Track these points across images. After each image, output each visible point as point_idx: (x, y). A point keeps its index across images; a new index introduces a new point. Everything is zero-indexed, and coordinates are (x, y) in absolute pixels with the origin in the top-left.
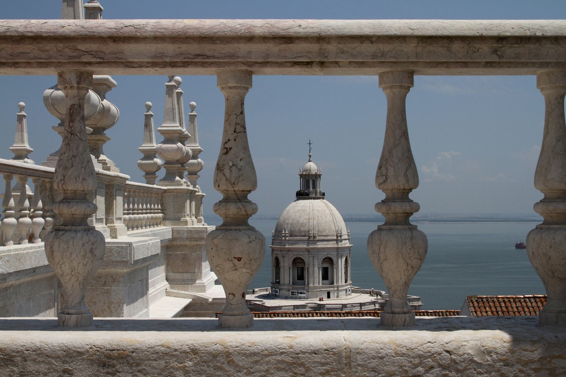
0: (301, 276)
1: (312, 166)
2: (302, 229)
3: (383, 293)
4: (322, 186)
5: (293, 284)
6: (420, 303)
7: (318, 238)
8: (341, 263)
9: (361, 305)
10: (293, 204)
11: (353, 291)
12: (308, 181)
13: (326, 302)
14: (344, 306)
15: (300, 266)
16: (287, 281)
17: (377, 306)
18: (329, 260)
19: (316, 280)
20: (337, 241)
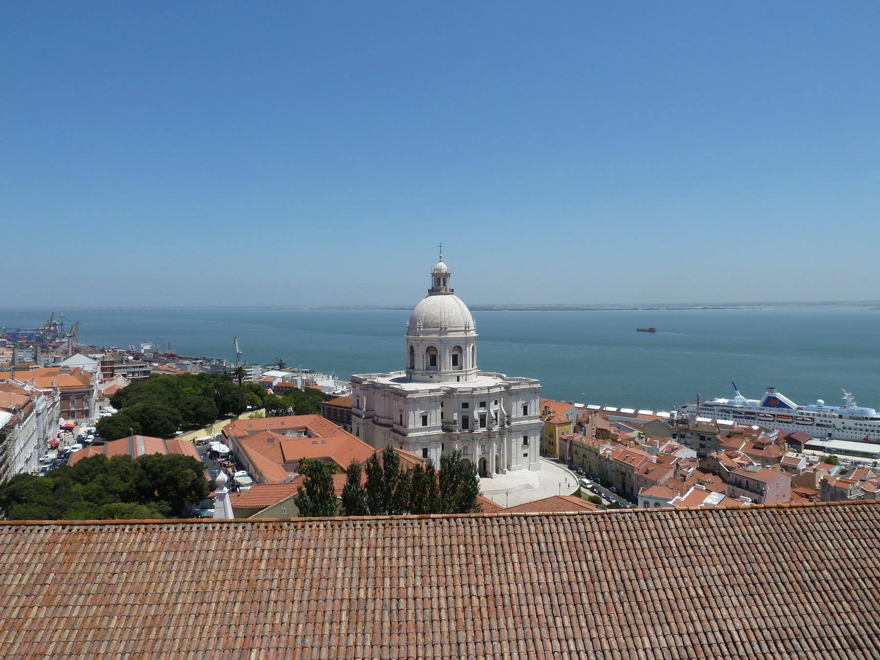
0: (433, 362)
1: (443, 266)
2: (435, 321)
3: (505, 376)
4: (450, 284)
5: (427, 369)
6: (539, 386)
7: (449, 329)
8: (469, 350)
9: (489, 388)
10: (424, 300)
11: (478, 374)
12: (439, 279)
13: (453, 384)
14: (474, 389)
15: (433, 353)
16: (421, 367)
17: (503, 389)
18: (459, 349)
19: (448, 366)
20: (466, 331)
